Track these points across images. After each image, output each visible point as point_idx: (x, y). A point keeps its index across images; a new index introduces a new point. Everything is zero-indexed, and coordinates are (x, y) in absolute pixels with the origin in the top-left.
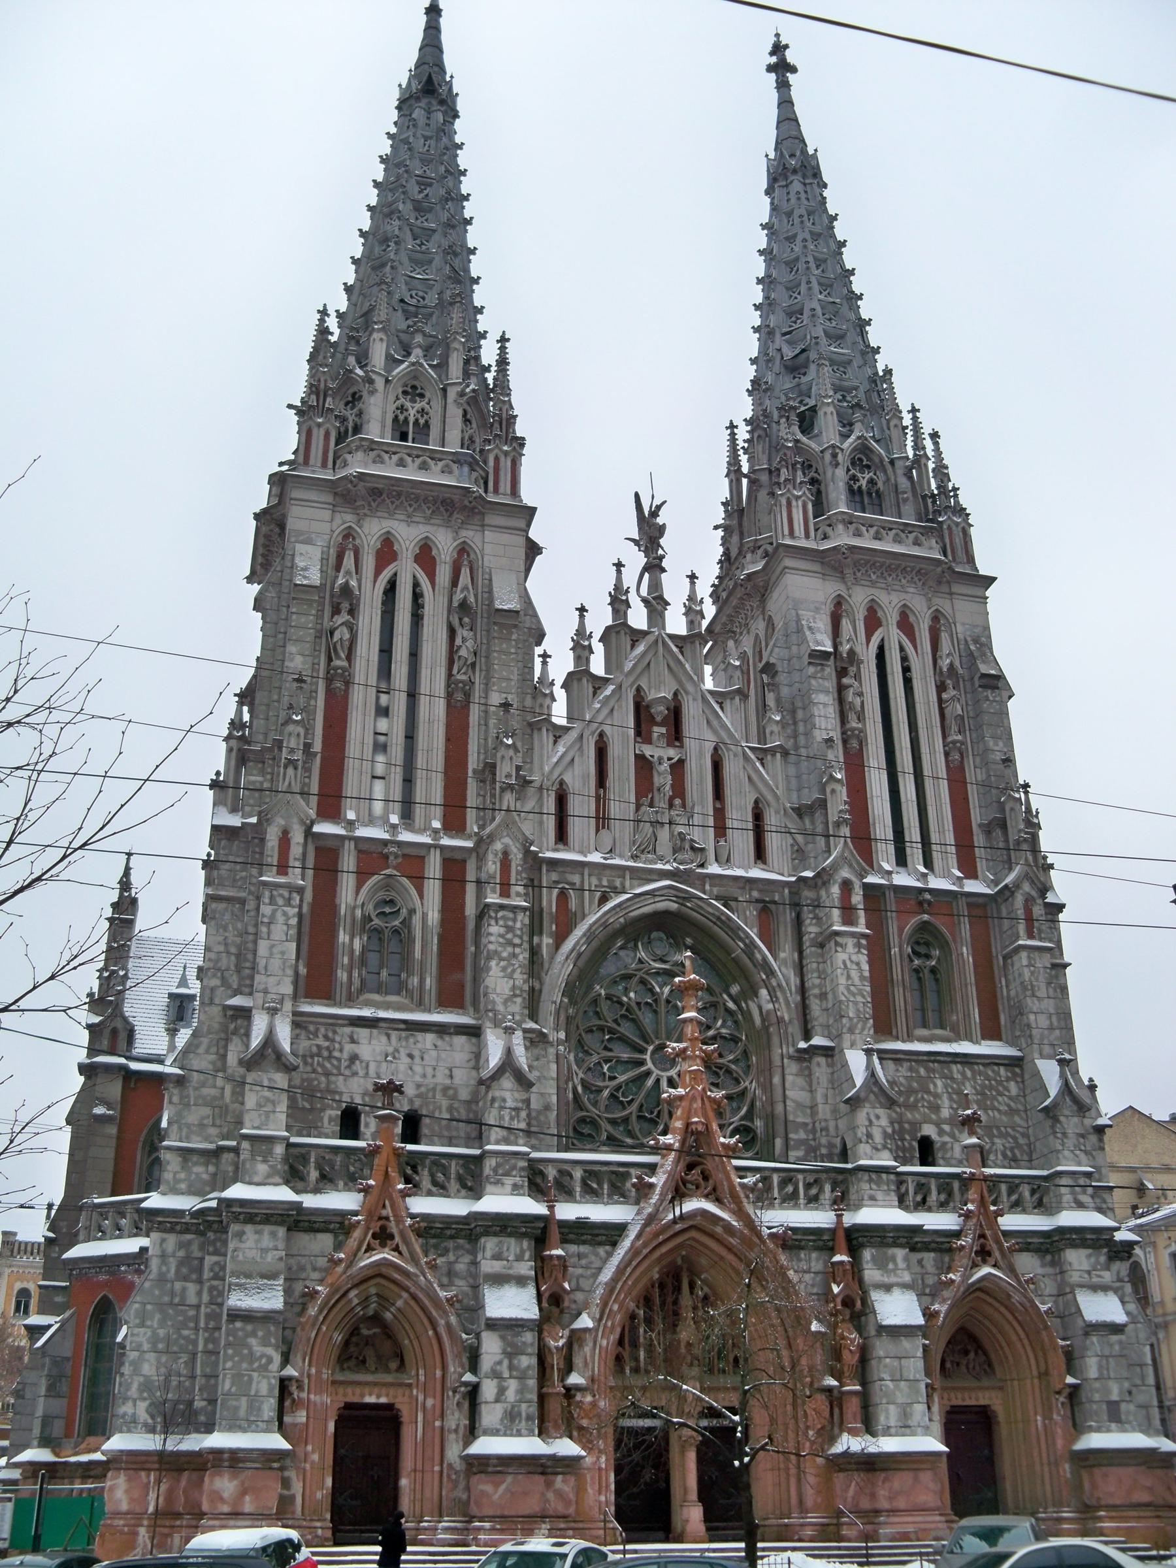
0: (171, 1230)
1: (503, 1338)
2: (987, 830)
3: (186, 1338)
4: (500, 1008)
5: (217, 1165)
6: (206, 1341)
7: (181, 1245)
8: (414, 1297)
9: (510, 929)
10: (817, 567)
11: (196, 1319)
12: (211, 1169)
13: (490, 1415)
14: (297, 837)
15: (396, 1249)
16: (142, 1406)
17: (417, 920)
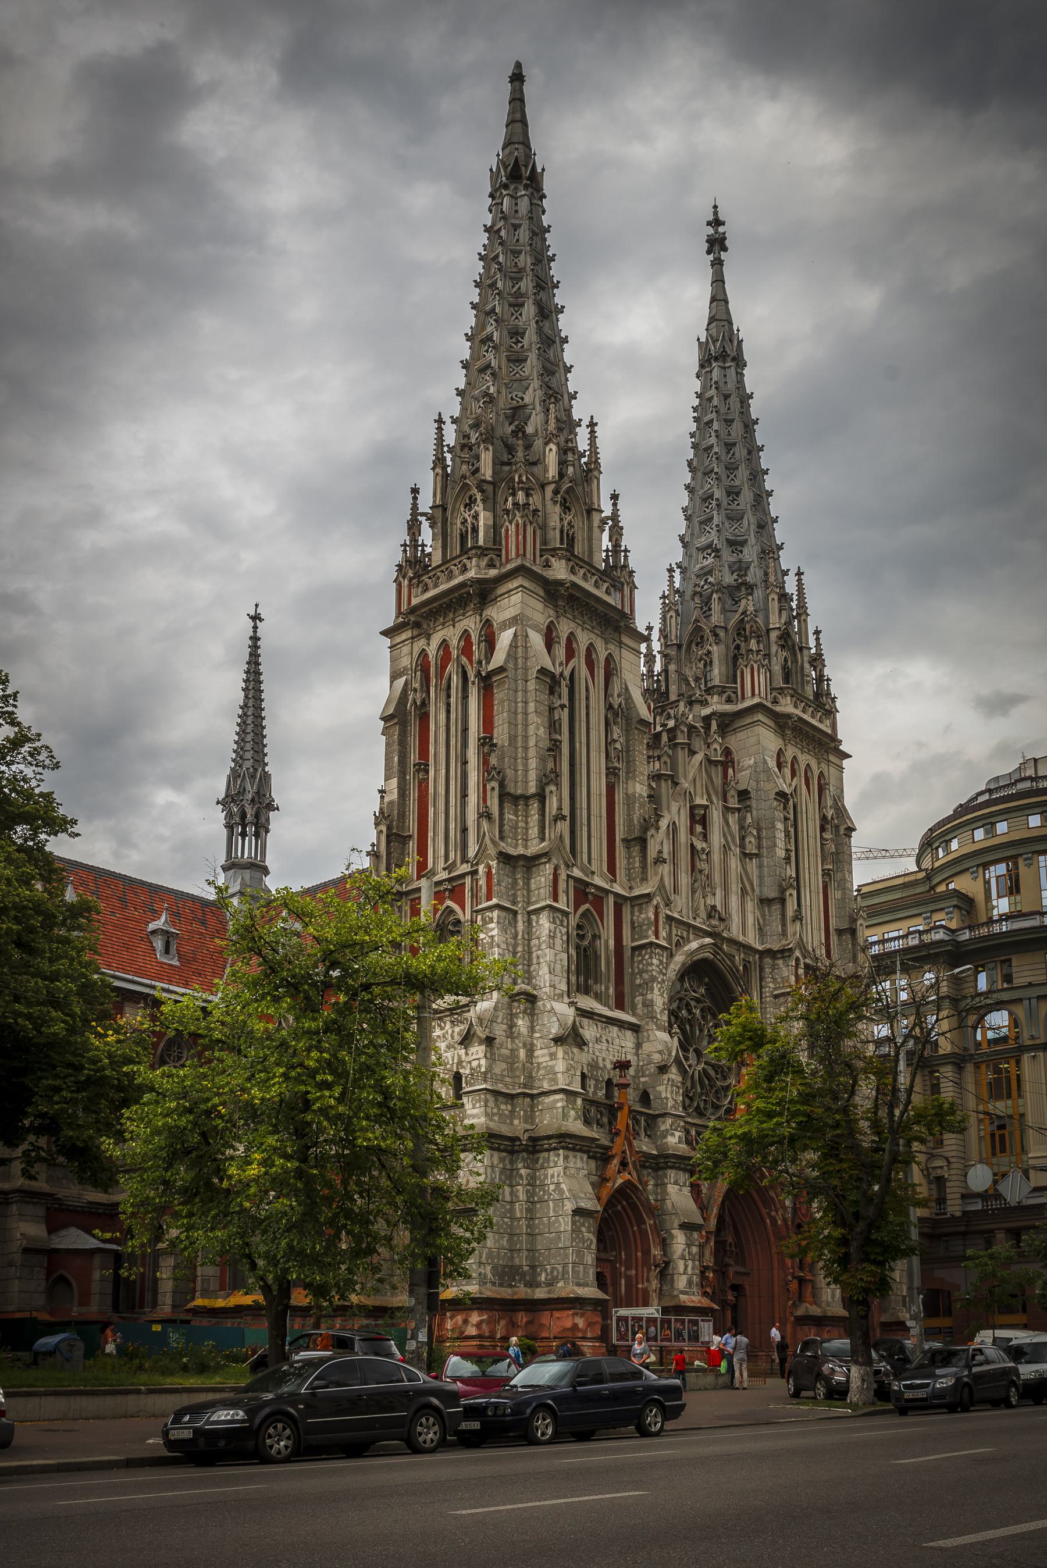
0: (498, 1149)
1: (685, 1235)
2: (840, 932)
3: (506, 1224)
4: (659, 1016)
5: (512, 1105)
6: (528, 1226)
7: (502, 1160)
8: (634, 1207)
9: (661, 962)
10: (771, 724)
11: (512, 1211)
12: (509, 1107)
13: (681, 1283)
14: (563, 877)
15: (629, 1173)
16: (489, 1268)
17: (600, 944)
